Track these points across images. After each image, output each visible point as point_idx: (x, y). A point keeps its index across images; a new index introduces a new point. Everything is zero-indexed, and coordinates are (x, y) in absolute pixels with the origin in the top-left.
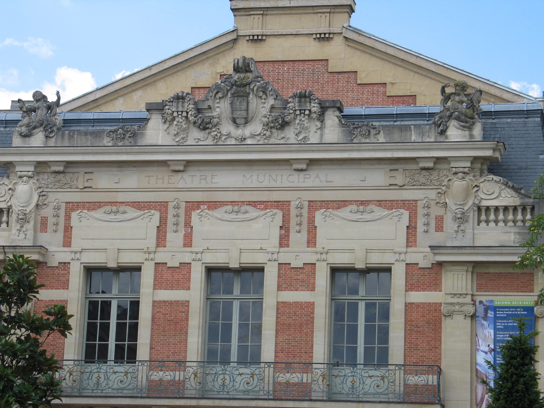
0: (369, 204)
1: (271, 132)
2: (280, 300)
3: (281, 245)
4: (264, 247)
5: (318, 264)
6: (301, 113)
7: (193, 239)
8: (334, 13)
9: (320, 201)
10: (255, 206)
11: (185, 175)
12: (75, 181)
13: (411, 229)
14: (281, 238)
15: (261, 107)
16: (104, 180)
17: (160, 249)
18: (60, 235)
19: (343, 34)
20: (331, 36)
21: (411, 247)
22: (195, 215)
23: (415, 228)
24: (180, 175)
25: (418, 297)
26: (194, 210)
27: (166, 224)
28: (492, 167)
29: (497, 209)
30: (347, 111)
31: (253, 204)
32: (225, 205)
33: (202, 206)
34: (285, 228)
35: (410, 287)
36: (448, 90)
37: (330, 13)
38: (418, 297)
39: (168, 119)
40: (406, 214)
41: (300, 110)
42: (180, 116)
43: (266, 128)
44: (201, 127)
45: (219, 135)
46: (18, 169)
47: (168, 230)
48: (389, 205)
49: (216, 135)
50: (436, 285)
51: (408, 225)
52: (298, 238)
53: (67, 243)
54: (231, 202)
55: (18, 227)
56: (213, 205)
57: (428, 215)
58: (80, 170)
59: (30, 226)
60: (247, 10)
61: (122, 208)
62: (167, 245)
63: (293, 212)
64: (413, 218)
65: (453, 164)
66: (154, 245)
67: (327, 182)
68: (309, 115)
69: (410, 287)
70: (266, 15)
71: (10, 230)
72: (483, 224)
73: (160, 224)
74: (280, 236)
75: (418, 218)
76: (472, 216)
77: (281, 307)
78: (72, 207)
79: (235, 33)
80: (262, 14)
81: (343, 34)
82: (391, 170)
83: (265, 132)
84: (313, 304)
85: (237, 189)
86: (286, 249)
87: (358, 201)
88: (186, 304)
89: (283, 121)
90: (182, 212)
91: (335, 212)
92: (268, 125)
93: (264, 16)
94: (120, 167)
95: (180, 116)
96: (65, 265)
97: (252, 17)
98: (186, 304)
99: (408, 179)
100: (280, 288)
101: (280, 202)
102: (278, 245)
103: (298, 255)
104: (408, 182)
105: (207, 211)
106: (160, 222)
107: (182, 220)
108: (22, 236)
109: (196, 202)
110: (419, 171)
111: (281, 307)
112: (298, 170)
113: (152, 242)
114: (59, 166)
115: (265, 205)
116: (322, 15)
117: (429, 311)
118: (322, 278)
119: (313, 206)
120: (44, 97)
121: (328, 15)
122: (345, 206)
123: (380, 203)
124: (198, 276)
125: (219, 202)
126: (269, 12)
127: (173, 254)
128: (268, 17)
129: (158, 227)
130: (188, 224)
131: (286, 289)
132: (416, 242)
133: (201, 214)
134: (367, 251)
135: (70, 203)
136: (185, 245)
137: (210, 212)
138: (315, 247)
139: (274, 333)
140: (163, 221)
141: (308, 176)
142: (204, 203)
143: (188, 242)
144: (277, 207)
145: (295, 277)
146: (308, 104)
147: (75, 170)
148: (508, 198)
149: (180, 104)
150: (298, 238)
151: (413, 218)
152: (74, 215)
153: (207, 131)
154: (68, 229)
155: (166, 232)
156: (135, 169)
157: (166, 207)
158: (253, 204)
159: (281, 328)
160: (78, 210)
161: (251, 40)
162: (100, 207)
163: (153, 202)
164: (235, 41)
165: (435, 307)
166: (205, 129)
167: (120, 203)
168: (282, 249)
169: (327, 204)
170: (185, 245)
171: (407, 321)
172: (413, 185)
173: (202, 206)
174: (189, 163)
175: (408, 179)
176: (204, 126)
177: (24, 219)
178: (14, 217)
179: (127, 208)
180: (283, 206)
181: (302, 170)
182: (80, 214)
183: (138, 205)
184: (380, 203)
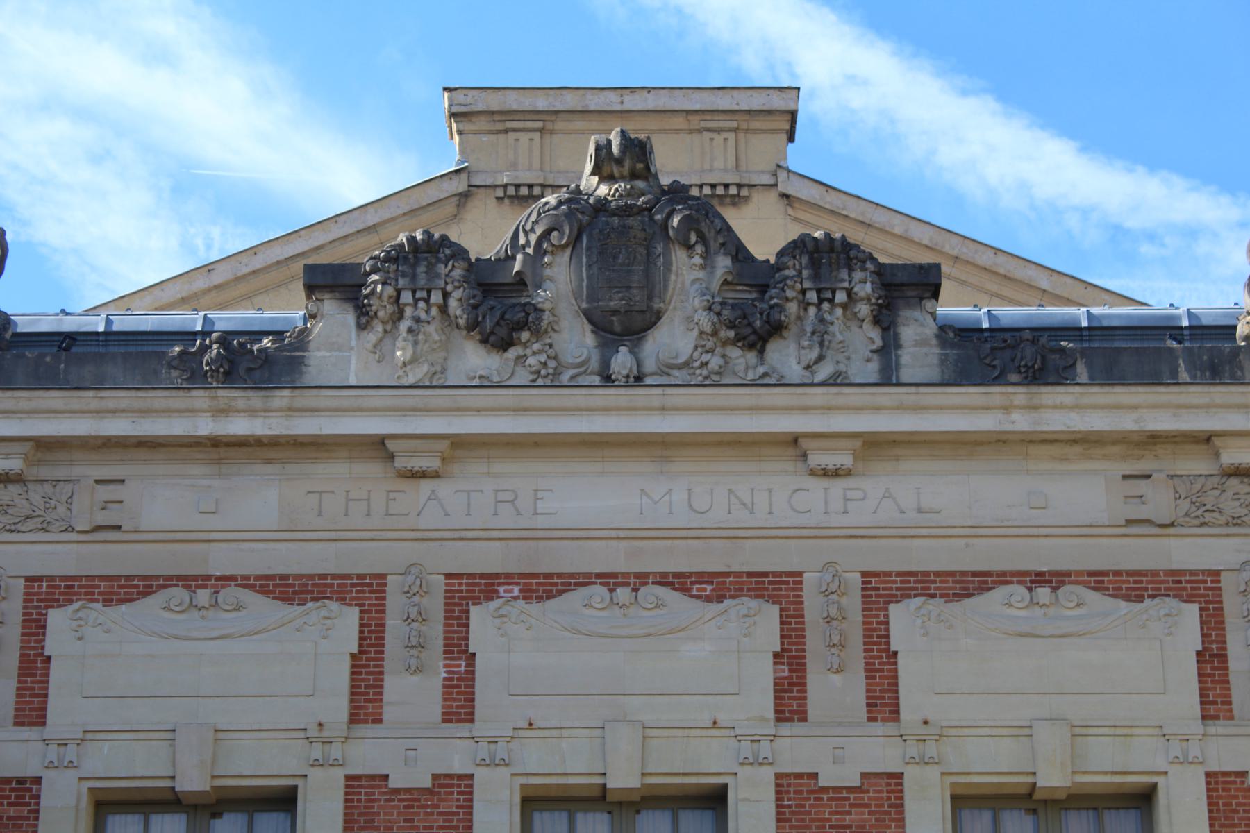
0: (1063, 583)
1: (724, 356)
3: (781, 716)
4: (723, 718)
5: (912, 776)
6: (821, 301)
7: (477, 696)
8: (747, 131)
9: (899, 574)
10: (684, 590)
11: (444, 488)
12: (62, 509)
13: (1212, 662)
15: (689, 280)
16: (165, 504)
17: (361, 730)
19: (781, 188)
20: (744, 192)
21: (1216, 717)
22: (479, 615)
23: (1223, 657)
24: (426, 486)
26: (477, 601)
27: (380, 644)
30: (954, 306)
31: (680, 582)
32: (576, 584)
33: (501, 589)
37: (735, 130)
39: (381, 314)
40: (1191, 612)
41: (819, 291)
42: (422, 304)
43: (709, 345)
44: (492, 339)
45: (552, 364)
47: (388, 665)
48: (1134, 586)
49: (545, 365)
51: (1200, 648)
52: (835, 688)
54: (599, 575)
56: (543, 587)
58: (77, 471)
60: (497, 118)
61: (231, 594)
62: (385, 717)
64: (1213, 623)
66: (344, 715)
67: (920, 511)
68: (844, 306)
70: (552, 132)
73: (360, 645)
74: (776, 684)
75: (1228, 626)
78: (46, 594)
79: (464, 176)
80: (541, 130)
81: (781, 188)
82: (1125, 477)
83: (706, 357)
85: (622, 534)
86: (797, 728)
87: (1027, 573)
89: (768, 322)
90: (435, 605)
91: (956, 607)
92: (715, 333)
93: (547, 136)
94: (219, 461)
95: (422, 304)
97: (512, 136)
99: (1185, 505)
101: (765, 574)
102: (771, 715)
104: (1187, 515)
105: (521, 603)
106: (361, 639)
107: (436, 632)
109: (482, 576)
110: (1216, 480)
112: (825, 473)
113: (337, 707)
114: (7, 456)
115: (717, 587)
116: (715, 135)
119: (881, 591)
121: (731, 136)
122: (984, 588)
123: (1098, 580)
125: (560, 575)
126: (560, 125)
127: (411, 743)
128: (556, 138)
129: (353, 656)
130: (457, 645)
132: (1230, 703)
133: (502, 612)
134: (1078, 731)
135: (39, 579)
136: (448, 717)
137: (534, 608)
138: (897, 720)
141: (859, 494)
142: (509, 578)
143: (460, 704)
146: (844, 274)
149: (421, 269)
150: (835, 688)
151: (1213, 623)
152: (57, 619)
153: (513, 353)
155: (382, 673)
156: (269, 468)
157: (381, 591)
158: (680, 582)
160: (71, 601)
161: (510, 197)
162: (148, 591)
163: (334, 577)
164: (464, 197)
166: (504, 345)
167: (219, 578)
168: (786, 729)
170: (448, 717)
172: (1203, 524)
173: (501, 589)
174: (461, 445)
175: (1185, 505)
176: (500, 339)
179: (247, 596)
180: (777, 588)
182: (80, 614)
183: (285, 589)
184: (1098, 580)
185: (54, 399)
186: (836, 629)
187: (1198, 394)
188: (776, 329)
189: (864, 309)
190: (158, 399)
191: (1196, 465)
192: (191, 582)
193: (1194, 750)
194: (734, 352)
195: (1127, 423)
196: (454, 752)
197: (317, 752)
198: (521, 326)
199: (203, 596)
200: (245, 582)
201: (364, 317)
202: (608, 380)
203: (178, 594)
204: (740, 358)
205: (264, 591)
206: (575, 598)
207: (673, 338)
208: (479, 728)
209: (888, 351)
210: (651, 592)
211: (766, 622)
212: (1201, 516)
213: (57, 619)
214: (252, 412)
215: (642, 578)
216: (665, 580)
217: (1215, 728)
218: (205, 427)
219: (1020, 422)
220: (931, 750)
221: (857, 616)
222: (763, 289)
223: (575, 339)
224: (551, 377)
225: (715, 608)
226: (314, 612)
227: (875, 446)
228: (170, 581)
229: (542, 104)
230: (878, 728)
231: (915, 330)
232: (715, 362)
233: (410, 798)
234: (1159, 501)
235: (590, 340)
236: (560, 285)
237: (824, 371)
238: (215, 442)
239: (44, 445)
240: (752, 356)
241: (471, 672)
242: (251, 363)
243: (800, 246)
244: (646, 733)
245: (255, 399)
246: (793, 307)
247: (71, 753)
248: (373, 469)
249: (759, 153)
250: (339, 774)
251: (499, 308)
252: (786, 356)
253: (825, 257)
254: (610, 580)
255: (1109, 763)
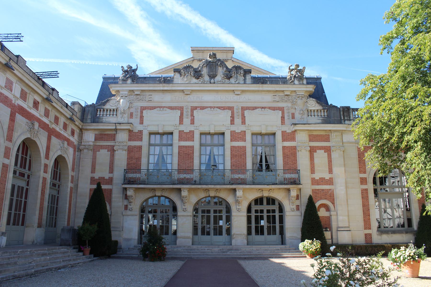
2: (232, 145)
3: (231, 124)
13: (283, 118)
14: (231, 121)
15: (221, 71)
16: (157, 98)
17: (181, 125)
18: (138, 120)
22: (195, 112)
23: (284, 117)
24: (188, 96)
25: (288, 144)
27: (183, 115)
28: (311, 96)
29: (314, 111)
30: (253, 74)
31: (219, 108)
34: (232, 117)
35: (284, 140)
36: (291, 68)
38: (288, 144)
46: (121, 93)
48: (274, 109)
50: (293, 139)
52: (238, 121)
53: (142, 122)
55: (121, 116)
56: (203, 108)
57: (289, 112)
58: (146, 94)
59: (126, 116)
61: (165, 109)
63: (235, 111)
64: (283, 113)
65: (298, 93)
69: (284, 140)
71: (118, 118)
72: (309, 116)
76: (306, 112)
77: (232, 148)
78: (143, 109)
84: (245, 147)
88: (193, 147)
90: (190, 110)
96: (141, 132)
98: (193, 147)
100: (231, 141)
103: (238, 128)
107: (190, 114)
108: (123, 119)
111: (232, 148)
115: (224, 108)
117: (292, 149)
118: (248, 137)
119: (244, 109)
120: (131, 67)
123: (270, 108)
124: (197, 136)
130: (192, 115)
131: (234, 141)
134: (267, 126)
136: (191, 124)
137: (201, 111)
139: (230, 158)
140: (182, 114)
142: (198, 107)
143: (192, 122)
144: (229, 109)
145: (235, 136)
147: (144, 94)
148: (319, 107)
150: (238, 121)
151: (283, 113)
152: (144, 112)
154: (142, 117)
157: (183, 108)
158: (219, 108)
159: (233, 156)
162: (155, 108)
164: (193, 60)
165: (295, 148)
166: (198, 79)
168: (232, 125)
169: (248, 108)
170: (191, 124)
171: (284, 153)
174: (192, 91)
176: (197, 78)
177: (124, 113)
178: (119, 112)
179: (167, 109)
180: (231, 108)
181: (238, 95)
183: (171, 108)
184: (270, 108)
185: (144, 85)
186: (238, 114)
187: (282, 86)
188: (231, 77)
189: (242, 75)
190: (156, 85)
191: (282, 94)
192: (160, 107)
193: (280, 128)
194: (226, 80)
195: (273, 89)
196: (192, 128)
197: (175, 128)
198: (200, 76)
199: (162, 109)
200: (167, 107)
201: (181, 75)
202: (211, 83)
203: (159, 109)
204: (227, 81)
205: (169, 108)
206: (206, 110)
207: (219, 78)
208: (195, 125)
209: (245, 80)
210: (215, 109)
211: (230, 112)
212: (282, 101)
213: (144, 111)
214: (167, 87)
215: (215, 107)
216: (217, 107)
217: (283, 126)
218: (162, 88)
219: (261, 89)
220: (249, 128)
221: (240, 112)
222: (230, 72)
223: (207, 78)
224: (203, 83)
225: (223, 111)
226: (175, 111)
227: (243, 91)
228: (158, 107)
229: (203, 49)
230: (243, 125)
231: (248, 77)
232: (224, 81)
233: (187, 133)
234: (277, 99)
235: (208, 78)
236: (205, 71)
237: (237, 82)
238: (163, 90)
239: (142, 91)
240: (228, 80)
241: (194, 118)
242: (167, 81)
243: (234, 67)
244: (215, 126)
245: (167, 85)
246: (233, 74)
247: (146, 128)
248: (182, 94)
249: (229, 55)
250: (178, 130)
251: (197, 74)
252: (232, 80)
253: (237, 68)
254: (211, 107)
255: (270, 130)
